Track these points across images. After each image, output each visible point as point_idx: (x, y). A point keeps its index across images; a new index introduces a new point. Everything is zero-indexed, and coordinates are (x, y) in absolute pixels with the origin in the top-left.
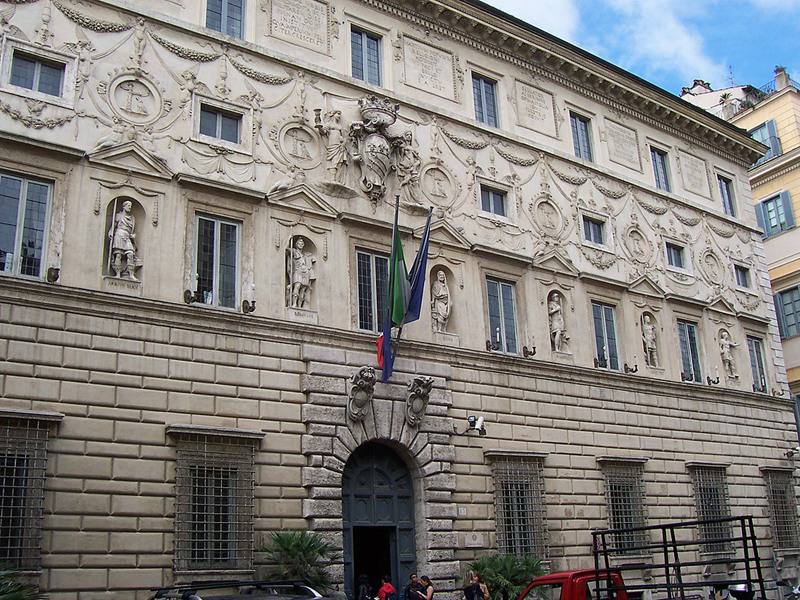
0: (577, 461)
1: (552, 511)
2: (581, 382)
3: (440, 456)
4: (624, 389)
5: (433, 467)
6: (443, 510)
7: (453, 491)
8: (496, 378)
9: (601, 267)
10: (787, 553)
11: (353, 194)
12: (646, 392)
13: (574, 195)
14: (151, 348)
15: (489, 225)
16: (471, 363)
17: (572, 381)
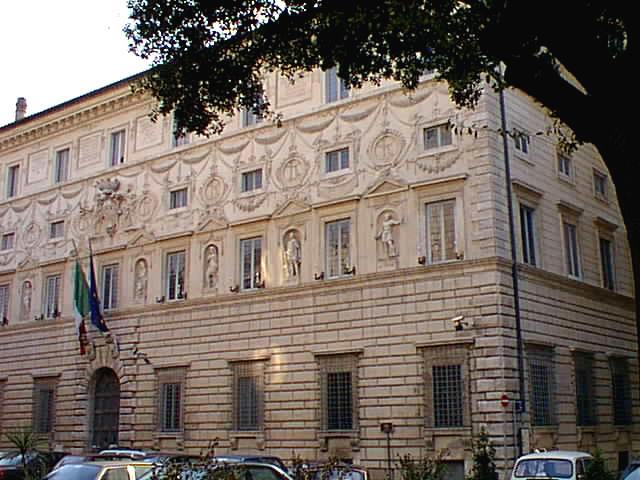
0: (213, 364)
1: (192, 400)
2: (223, 307)
3: (127, 372)
4: (259, 302)
5: (125, 379)
6: (127, 403)
7: (134, 392)
8: (164, 319)
9: (250, 209)
10: (436, 433)
11: (102, 238)
12: (280, 299)
13: (237, 161)
14: (33, 343)
15: (171, 218)
16: (151, 313)
17: (216, 308)
